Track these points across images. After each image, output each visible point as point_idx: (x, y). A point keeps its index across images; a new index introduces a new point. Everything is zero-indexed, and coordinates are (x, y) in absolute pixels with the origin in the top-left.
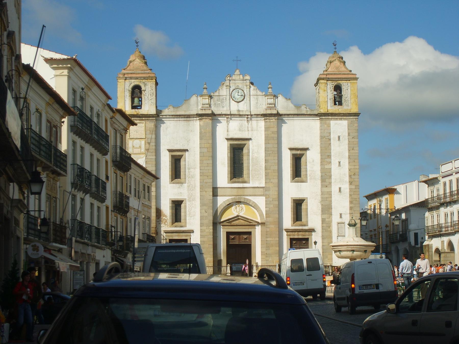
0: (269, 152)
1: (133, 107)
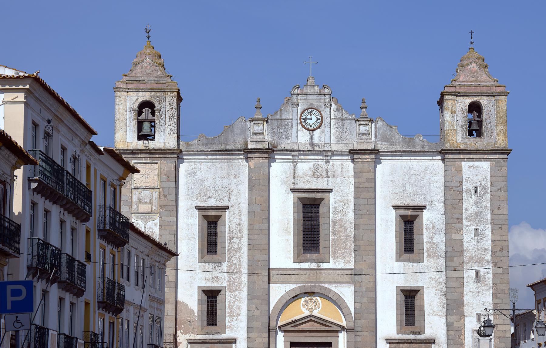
0: (361, 212)
1: (141, 137)
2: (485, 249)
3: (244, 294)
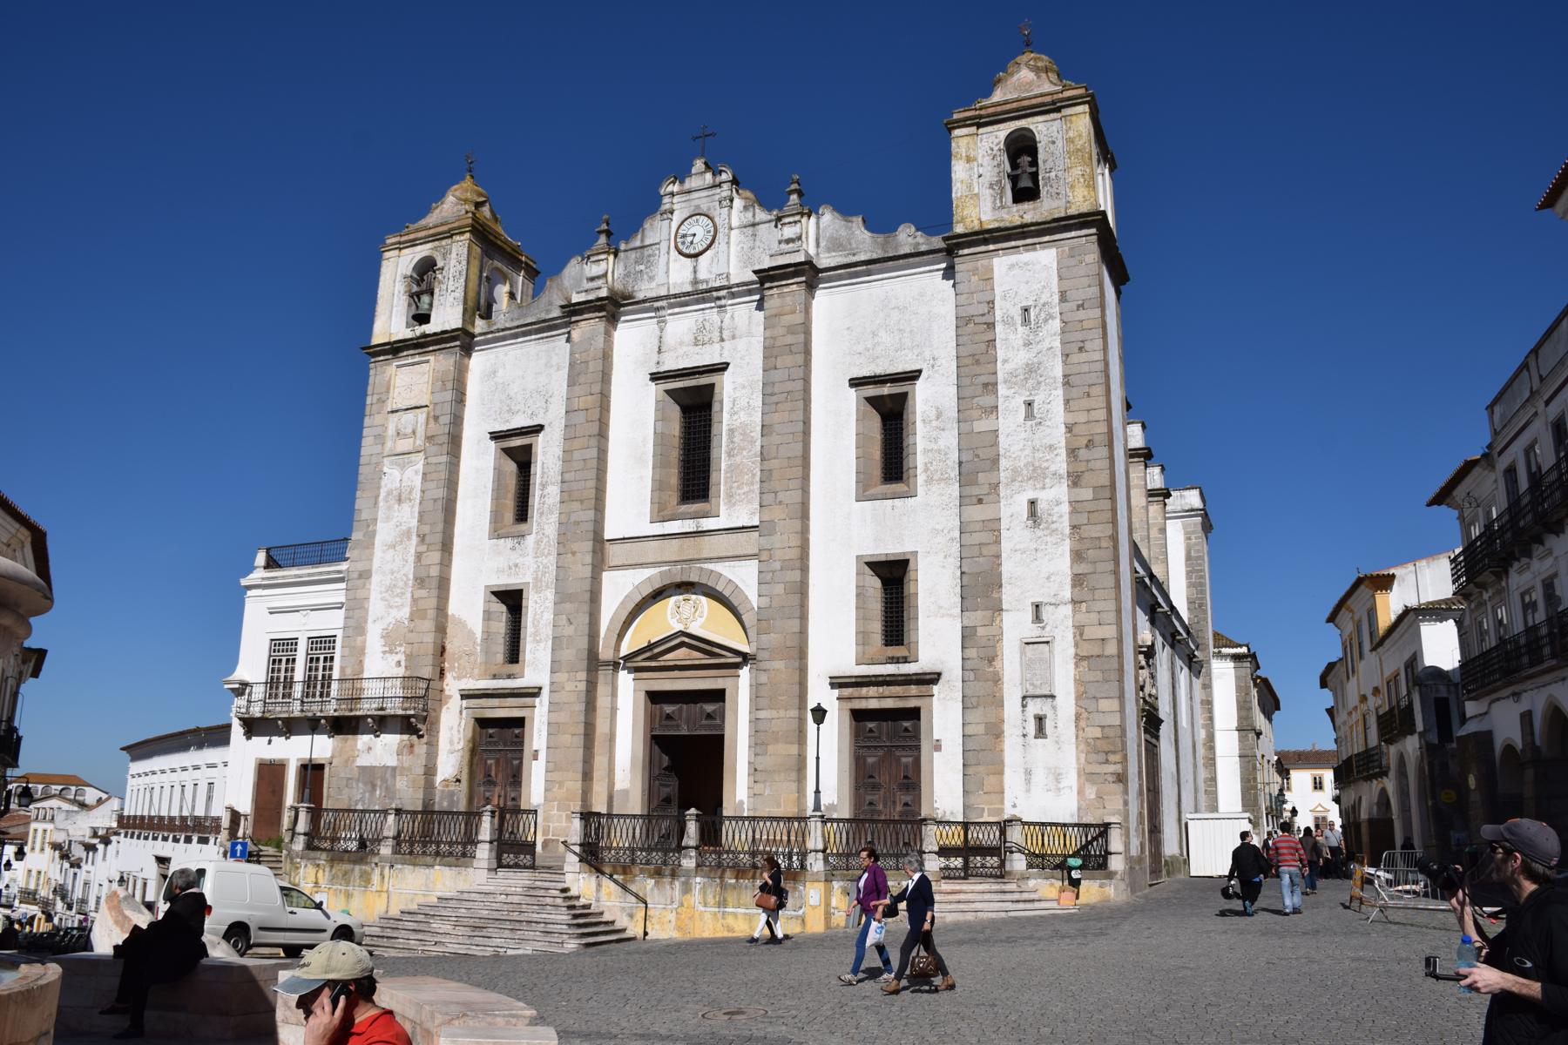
0: (775, 399)
2: (1051, 447)
3: (550, 595)
